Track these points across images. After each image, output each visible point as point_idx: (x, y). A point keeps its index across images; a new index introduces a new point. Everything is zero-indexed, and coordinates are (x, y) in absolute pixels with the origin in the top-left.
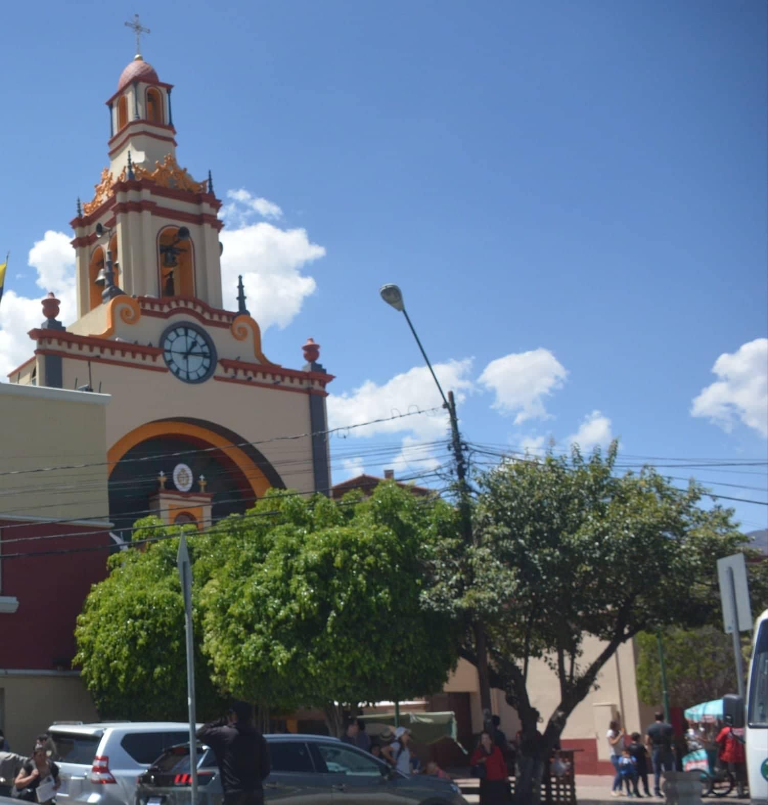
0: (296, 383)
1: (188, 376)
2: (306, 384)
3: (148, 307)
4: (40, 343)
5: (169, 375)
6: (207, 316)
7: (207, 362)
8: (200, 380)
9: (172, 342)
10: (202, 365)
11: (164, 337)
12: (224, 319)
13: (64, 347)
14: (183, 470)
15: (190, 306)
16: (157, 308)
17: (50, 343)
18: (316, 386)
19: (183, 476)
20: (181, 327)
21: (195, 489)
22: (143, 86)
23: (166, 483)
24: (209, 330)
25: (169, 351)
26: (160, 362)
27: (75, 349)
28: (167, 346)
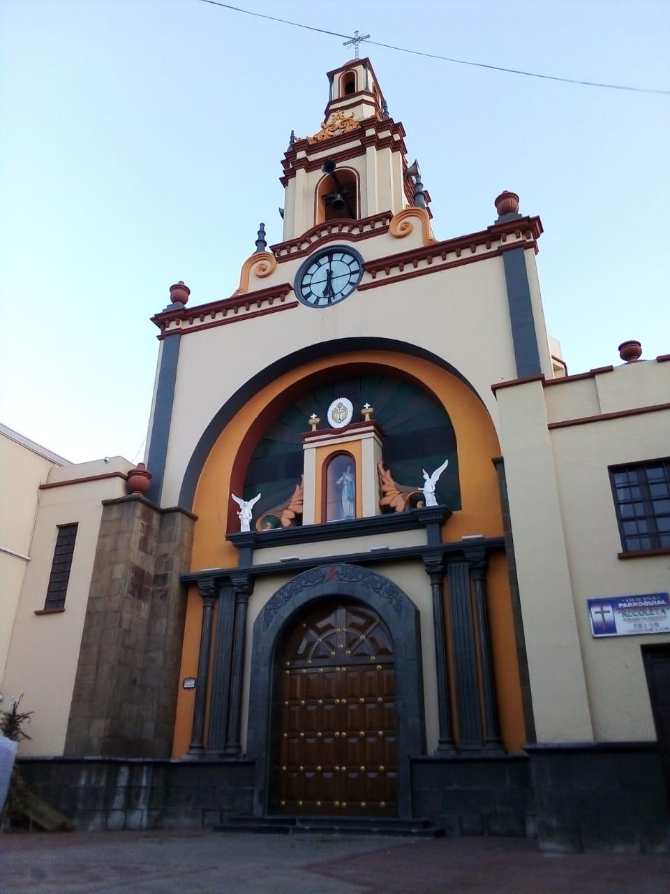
0: (481, 250)
1: (330, 301)
2: (495, 247)
3: (284, 253)
4: (163, 330)
5: (301, 306)
6: (356, 232)
7: (354, 278)
8: (344, 297)
9: (312, 275)
10: (349, 282)
11: (304, 271)
12: (379, 225)
13: (185, 325)
14: (340, 405)
15: (335, 230)
16: (294, 250)
17: (168, 327)
18: (511, 239)
19: (340, 411)
20: (322, 256)
21: (357, 420)
22: (337, 77)
23: (318, 425)
24: (357, 246)
25: (309, 285)
26: (291, 297)
27: (197, 322)
28: (306, 280)
